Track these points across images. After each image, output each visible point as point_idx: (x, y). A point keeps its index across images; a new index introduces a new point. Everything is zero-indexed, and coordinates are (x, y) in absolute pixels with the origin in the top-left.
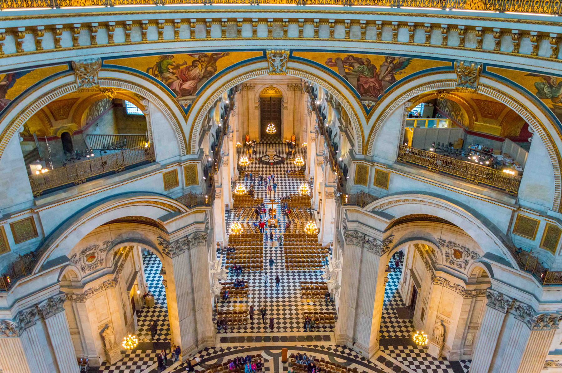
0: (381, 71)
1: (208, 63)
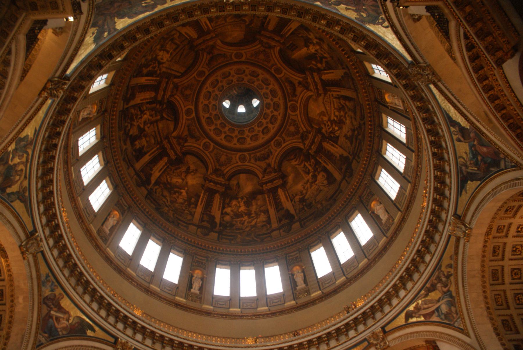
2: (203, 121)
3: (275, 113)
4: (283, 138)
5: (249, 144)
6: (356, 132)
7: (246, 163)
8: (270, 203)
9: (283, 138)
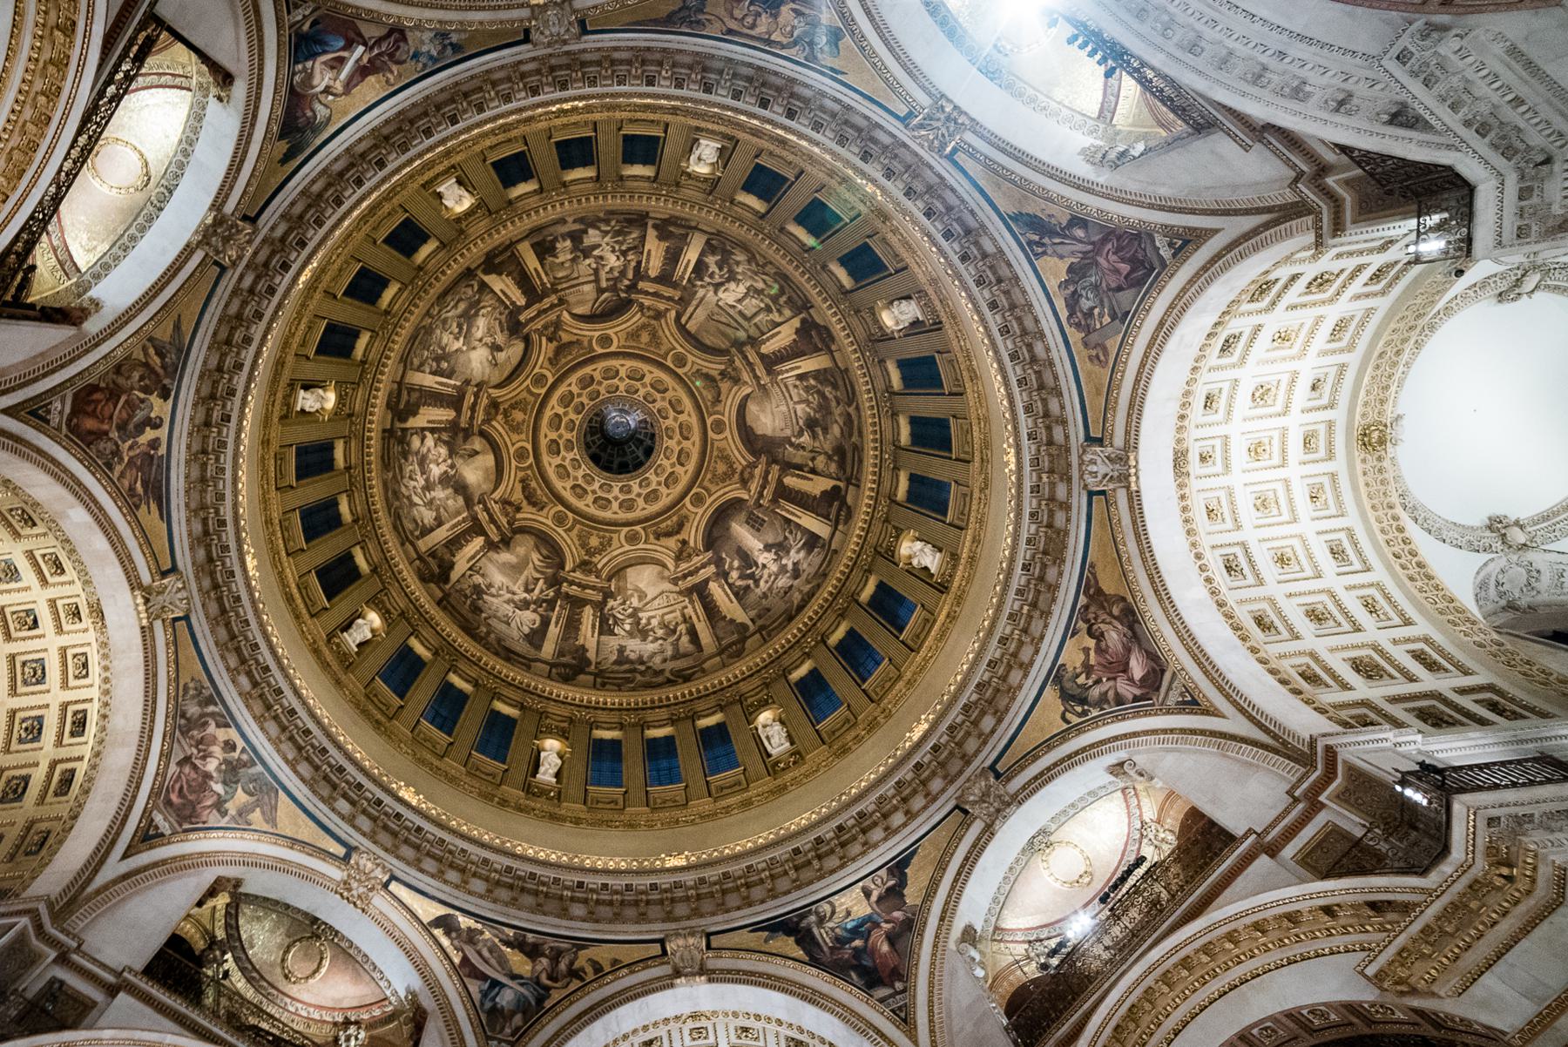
0: (1073, 253)
1: (1104, 608)
2: (588, 370)
3: (615, 505)
5: (550, 463)
6: (642, 668)
7: (514, 463)
8: (455, 526)
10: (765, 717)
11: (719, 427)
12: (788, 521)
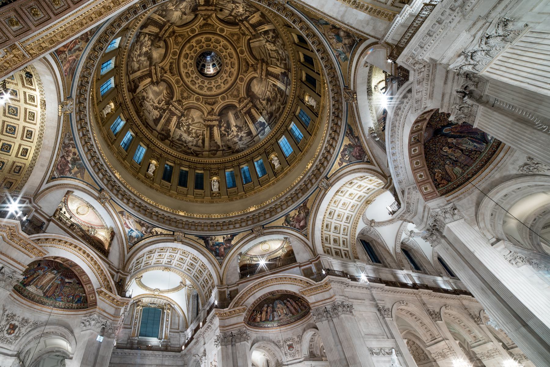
3: (197, 85)
4: (181, 86)
5: (183, 61)
6: (185, 145)
7: (171, 55)
9: (181, 86)
10: (215, 178)
11: (242, 80)
12: (246, 122)
